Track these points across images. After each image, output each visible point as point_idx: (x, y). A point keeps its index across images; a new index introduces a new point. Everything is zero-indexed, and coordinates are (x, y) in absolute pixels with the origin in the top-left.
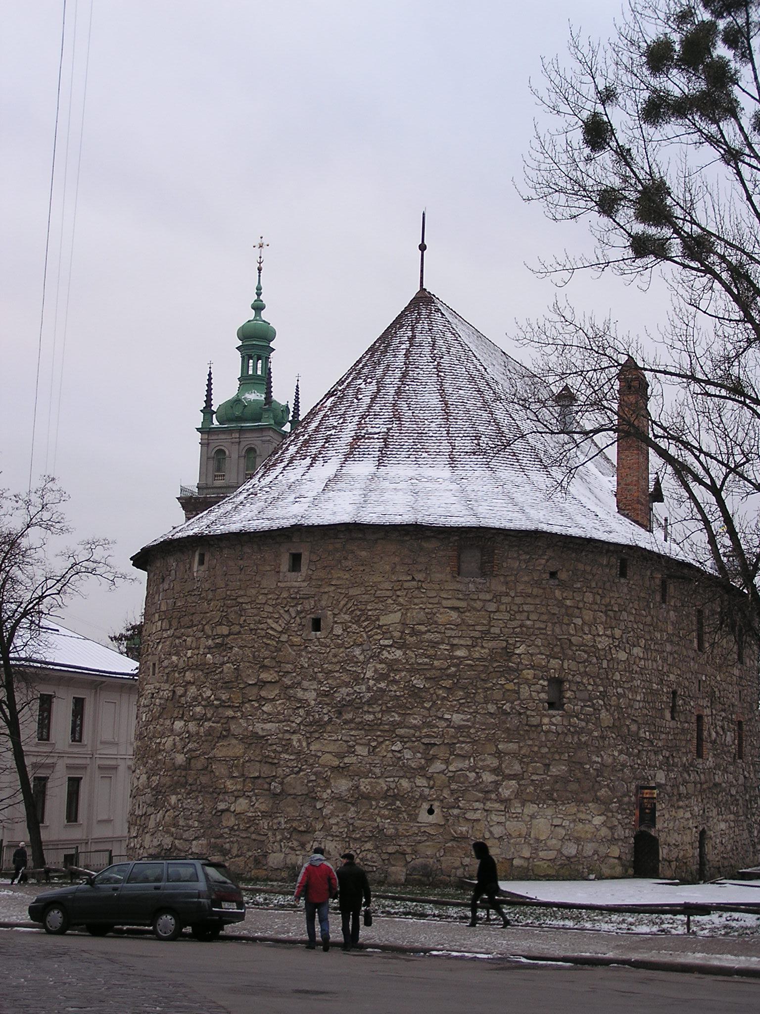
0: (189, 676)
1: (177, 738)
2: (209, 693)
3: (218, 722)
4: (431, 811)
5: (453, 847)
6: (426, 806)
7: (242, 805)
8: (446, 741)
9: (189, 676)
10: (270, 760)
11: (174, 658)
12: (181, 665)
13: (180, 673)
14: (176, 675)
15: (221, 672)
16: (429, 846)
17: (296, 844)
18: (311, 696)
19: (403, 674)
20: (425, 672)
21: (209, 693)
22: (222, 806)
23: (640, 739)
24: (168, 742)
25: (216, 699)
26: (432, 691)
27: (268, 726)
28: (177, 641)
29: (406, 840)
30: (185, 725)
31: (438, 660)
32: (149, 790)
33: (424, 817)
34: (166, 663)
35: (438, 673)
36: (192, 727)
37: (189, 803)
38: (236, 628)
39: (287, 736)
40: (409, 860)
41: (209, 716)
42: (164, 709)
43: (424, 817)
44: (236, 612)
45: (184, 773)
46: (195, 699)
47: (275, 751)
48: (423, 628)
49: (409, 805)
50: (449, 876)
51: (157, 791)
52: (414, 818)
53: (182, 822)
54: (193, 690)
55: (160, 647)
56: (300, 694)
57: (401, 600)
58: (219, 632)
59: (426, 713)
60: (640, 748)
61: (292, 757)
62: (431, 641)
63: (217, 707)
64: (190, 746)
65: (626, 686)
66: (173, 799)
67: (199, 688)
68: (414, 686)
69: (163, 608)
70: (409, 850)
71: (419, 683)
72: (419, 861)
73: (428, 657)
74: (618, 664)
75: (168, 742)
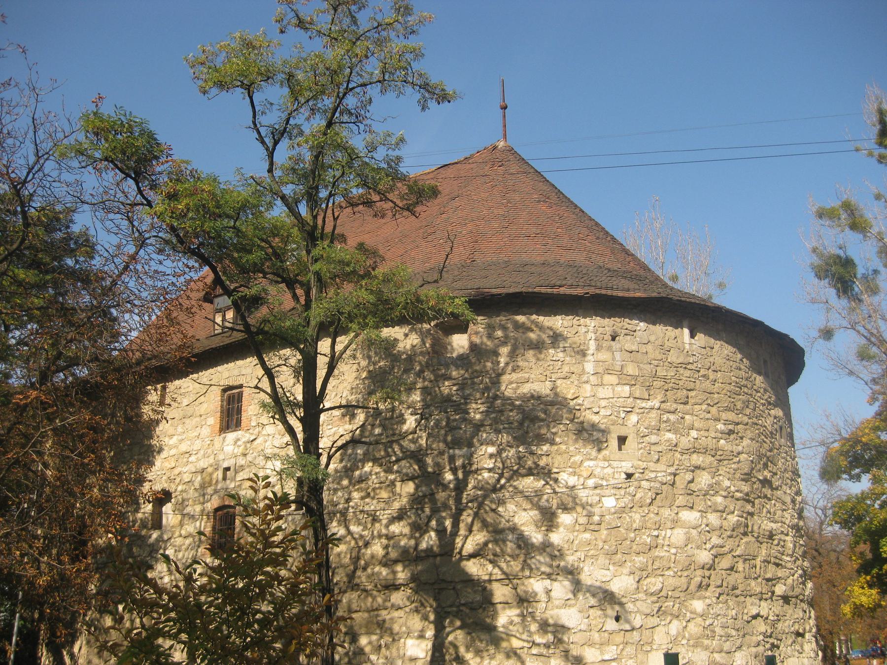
0: (697, 459)
1: (694, 532)
2: (727, 483)
3: (742, 517)
7: (764, 608)
9: (697, 459)
10: (777, 561)
11: (669, 435)
12: (685, 442)
13: (682, 454)
14: (677, 455)
15: (739, 462)
17: (798, 647)
18: (788, 499)
21: (727, 483)
22: (754, 612)
24: (678, 536)
25: (737, 491)
27: (774, 526)
28: (672, 417)
30: (702, 517)
32: (642, 596)
34: (653, 438)
36: (713, 519)
37: (719, 608)
38: (746, 419)
39: (783, 537)
41: (732, 508)
42: (657, 494)
44: (744, 402)
45: (707, 573)
46: (711, 486)
47: (779, 552)
51: (659, 595)
53: (718, 630)
54: (704, 480)
55: (634, 418)
56: (784, 497)
58: (730, 418)
61: (788, 559)
63: (738, 500)
64: (715, 540)
66: (698, 605)
67: (714, 475)
69: (631, 369)
75: (678, 536)
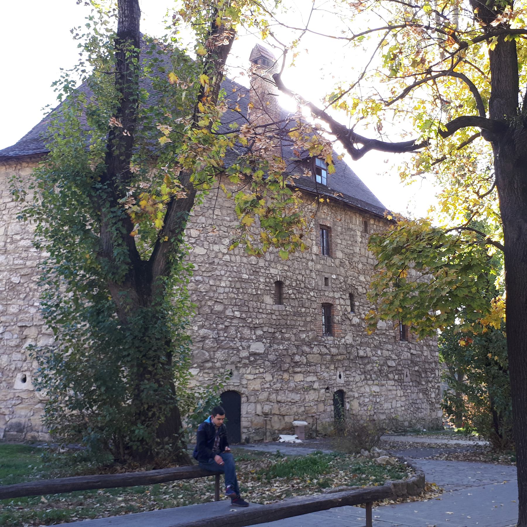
4: (24, 380)
5: (39, 408)
6: (20, 376)
8: (35, 324)
16: (22, 408)
19: (5, 273)
20: (20, 271)
23: (227, 317)
26: (26, 285)
29: (5, 403)
31: (30, 260)
33: (19, 385)
35: (29, 271)
40: (7, 419)
43: (19, 385)
48: (18, 237)
49: (8, 376)
50: (38, 432)
52: (10, 386)
57: (4, 217)
59: (21, 302)
60: (226, 324)
62: (24, 246)
65: (205, 274)
68: (11, 282)
70: (7, 412)
71: (15, 279)
72: (14, 421)
73: (22, 259)
74: (195, 257)
